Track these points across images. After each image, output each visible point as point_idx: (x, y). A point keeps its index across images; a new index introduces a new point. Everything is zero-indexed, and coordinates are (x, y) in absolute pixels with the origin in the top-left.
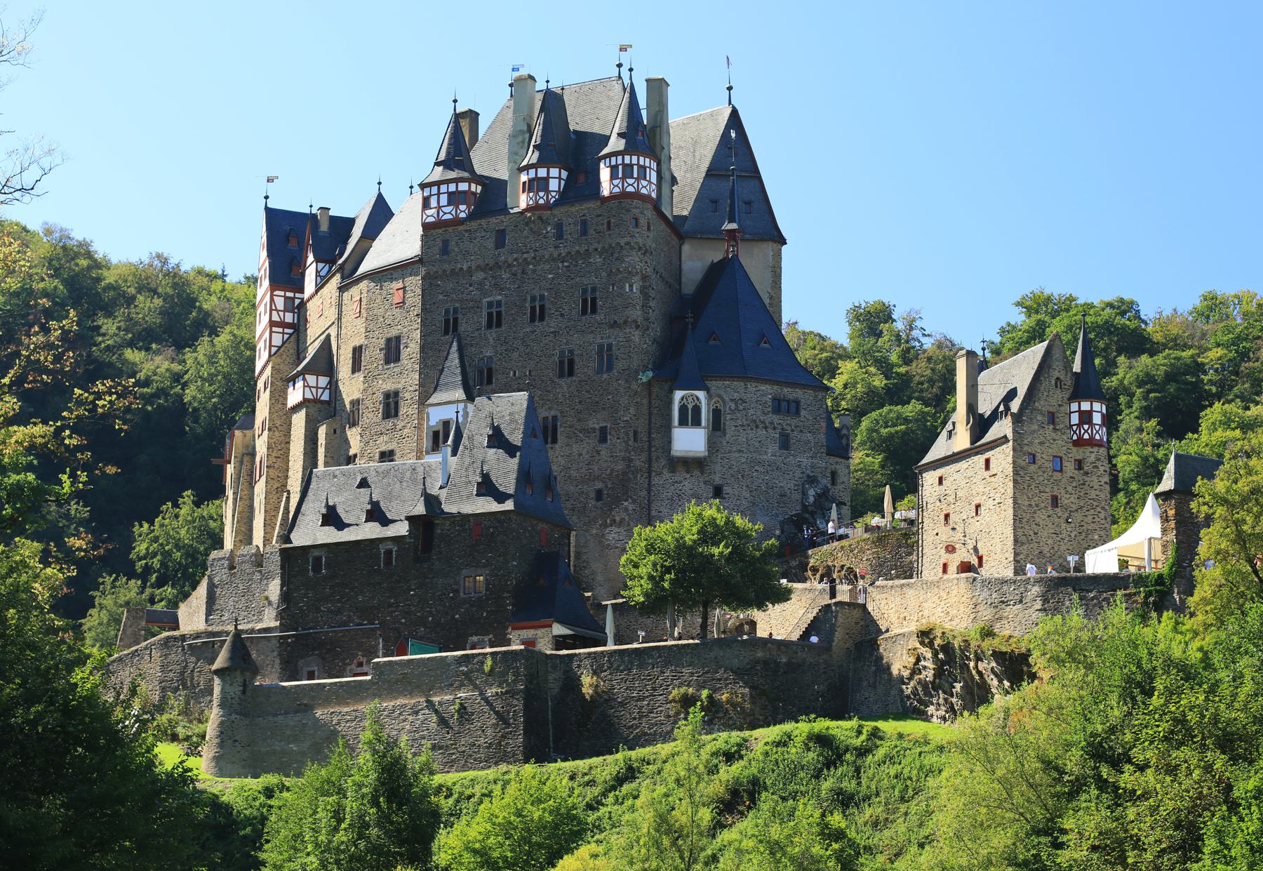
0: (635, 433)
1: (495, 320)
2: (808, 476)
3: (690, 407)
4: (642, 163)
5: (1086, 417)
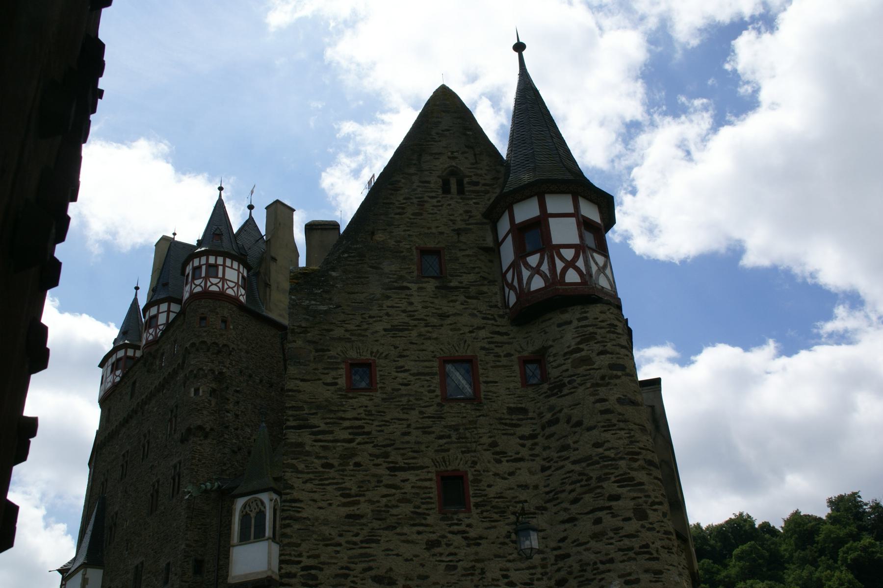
0: (199, 566)
3: (253, 515)
4: (212, 260)
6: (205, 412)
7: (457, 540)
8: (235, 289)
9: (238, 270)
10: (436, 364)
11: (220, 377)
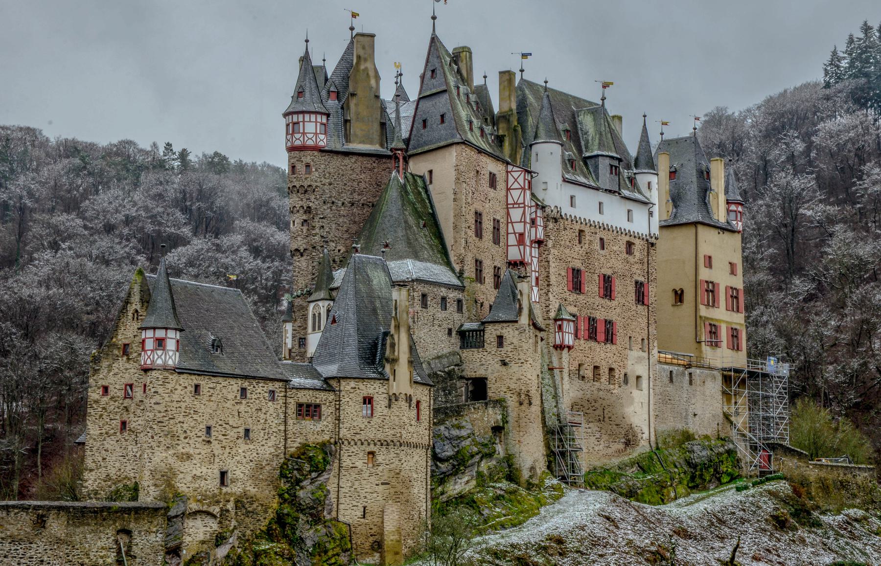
3: (317, 315)
4: (295, 120)
8: (314, 139)
9: (316, 122)
10: (123, 386)
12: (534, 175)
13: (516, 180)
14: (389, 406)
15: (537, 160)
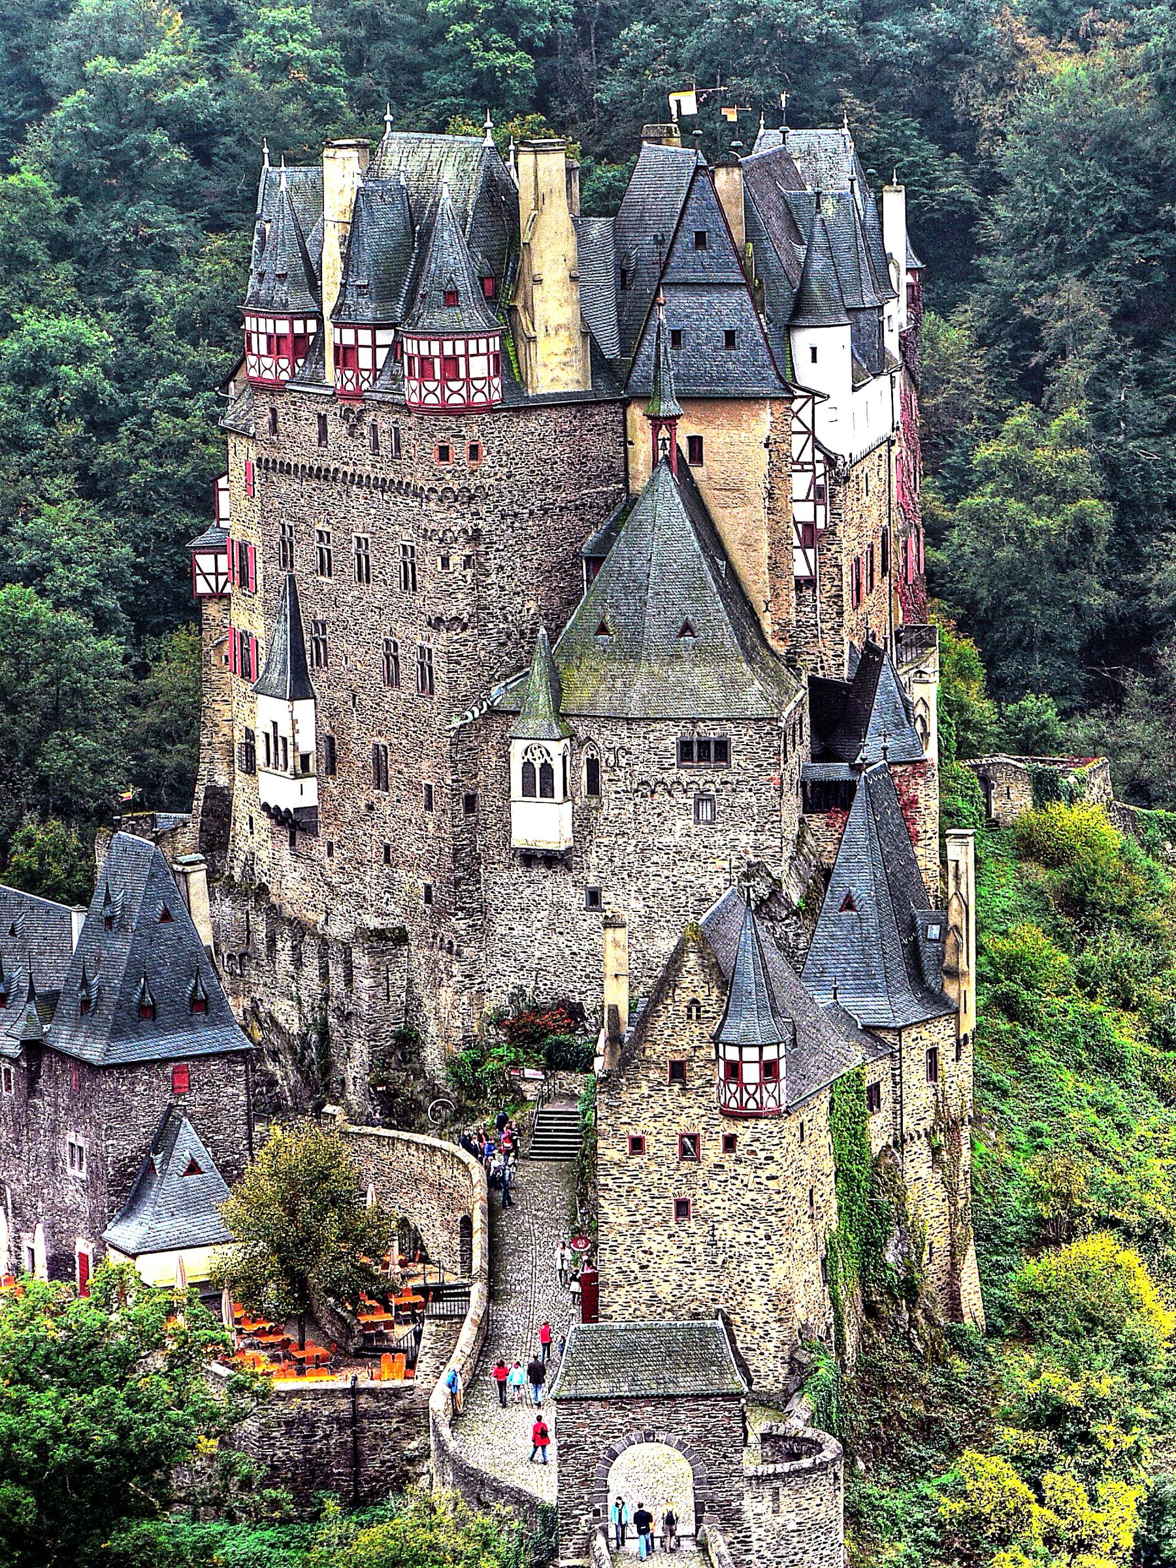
0: (470, 803)
1: (325, 567)
2: (749, 865)
3: (537, 766)
4: (448, 350)
5: (734, 1070)
6: (460, 596)
7: (683, 1234)
9: (487, 354)
10: (677, 1138)
11: (476, 537)
12: (817, 399)
13: (795, 415)
14: (958, 1058)
15: (814, 360)
